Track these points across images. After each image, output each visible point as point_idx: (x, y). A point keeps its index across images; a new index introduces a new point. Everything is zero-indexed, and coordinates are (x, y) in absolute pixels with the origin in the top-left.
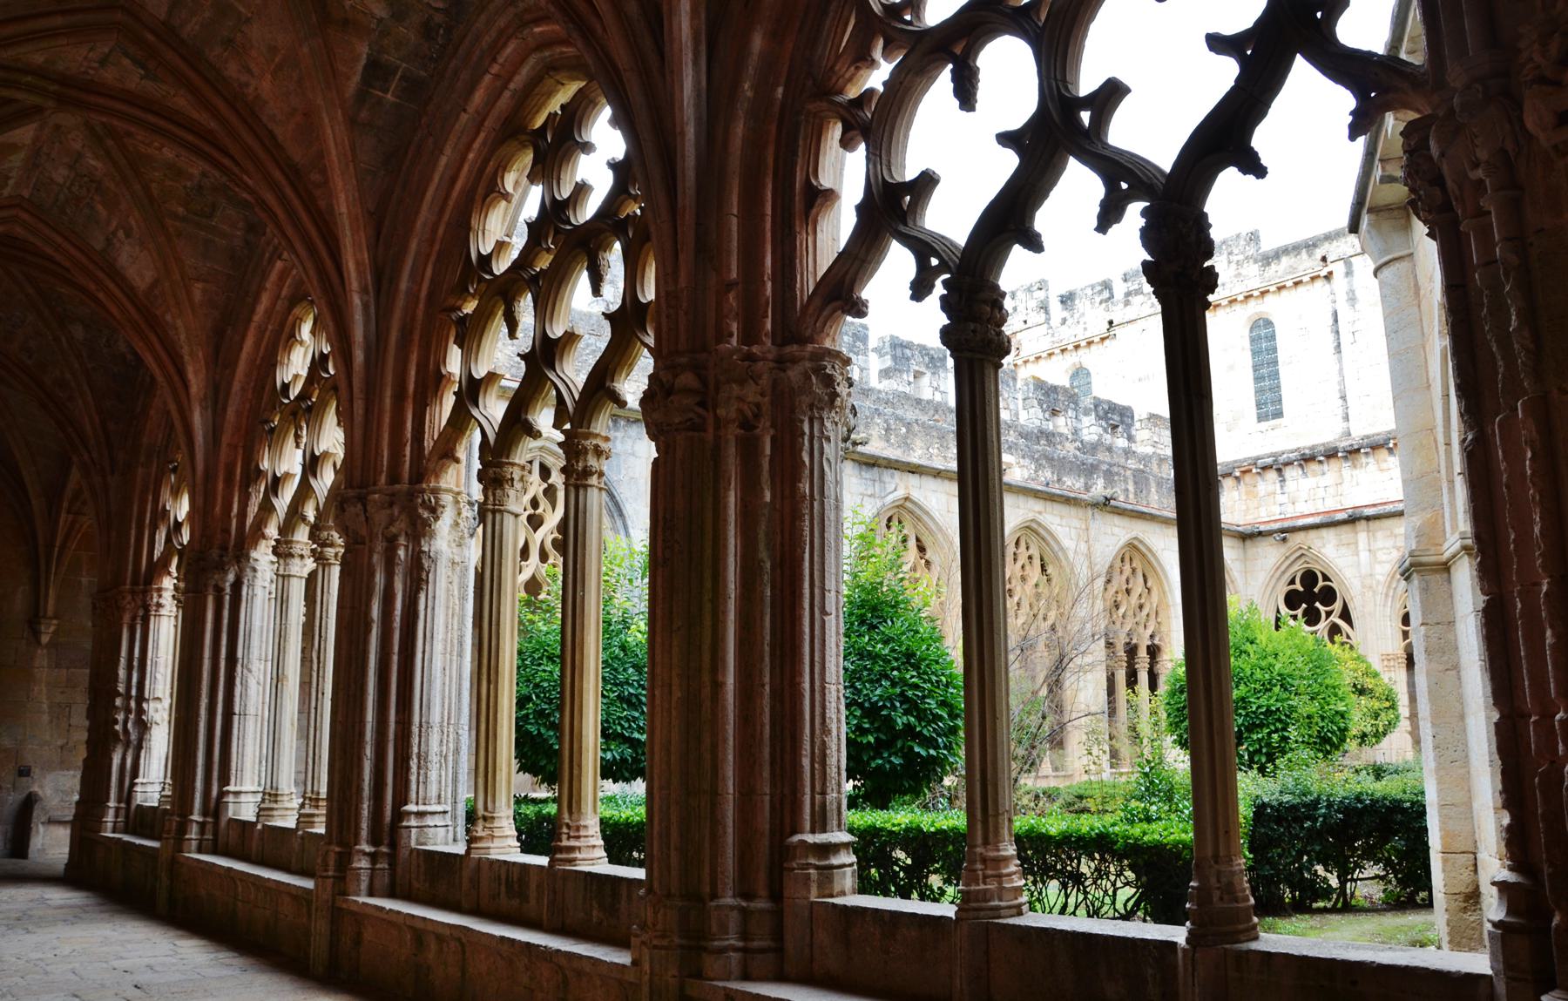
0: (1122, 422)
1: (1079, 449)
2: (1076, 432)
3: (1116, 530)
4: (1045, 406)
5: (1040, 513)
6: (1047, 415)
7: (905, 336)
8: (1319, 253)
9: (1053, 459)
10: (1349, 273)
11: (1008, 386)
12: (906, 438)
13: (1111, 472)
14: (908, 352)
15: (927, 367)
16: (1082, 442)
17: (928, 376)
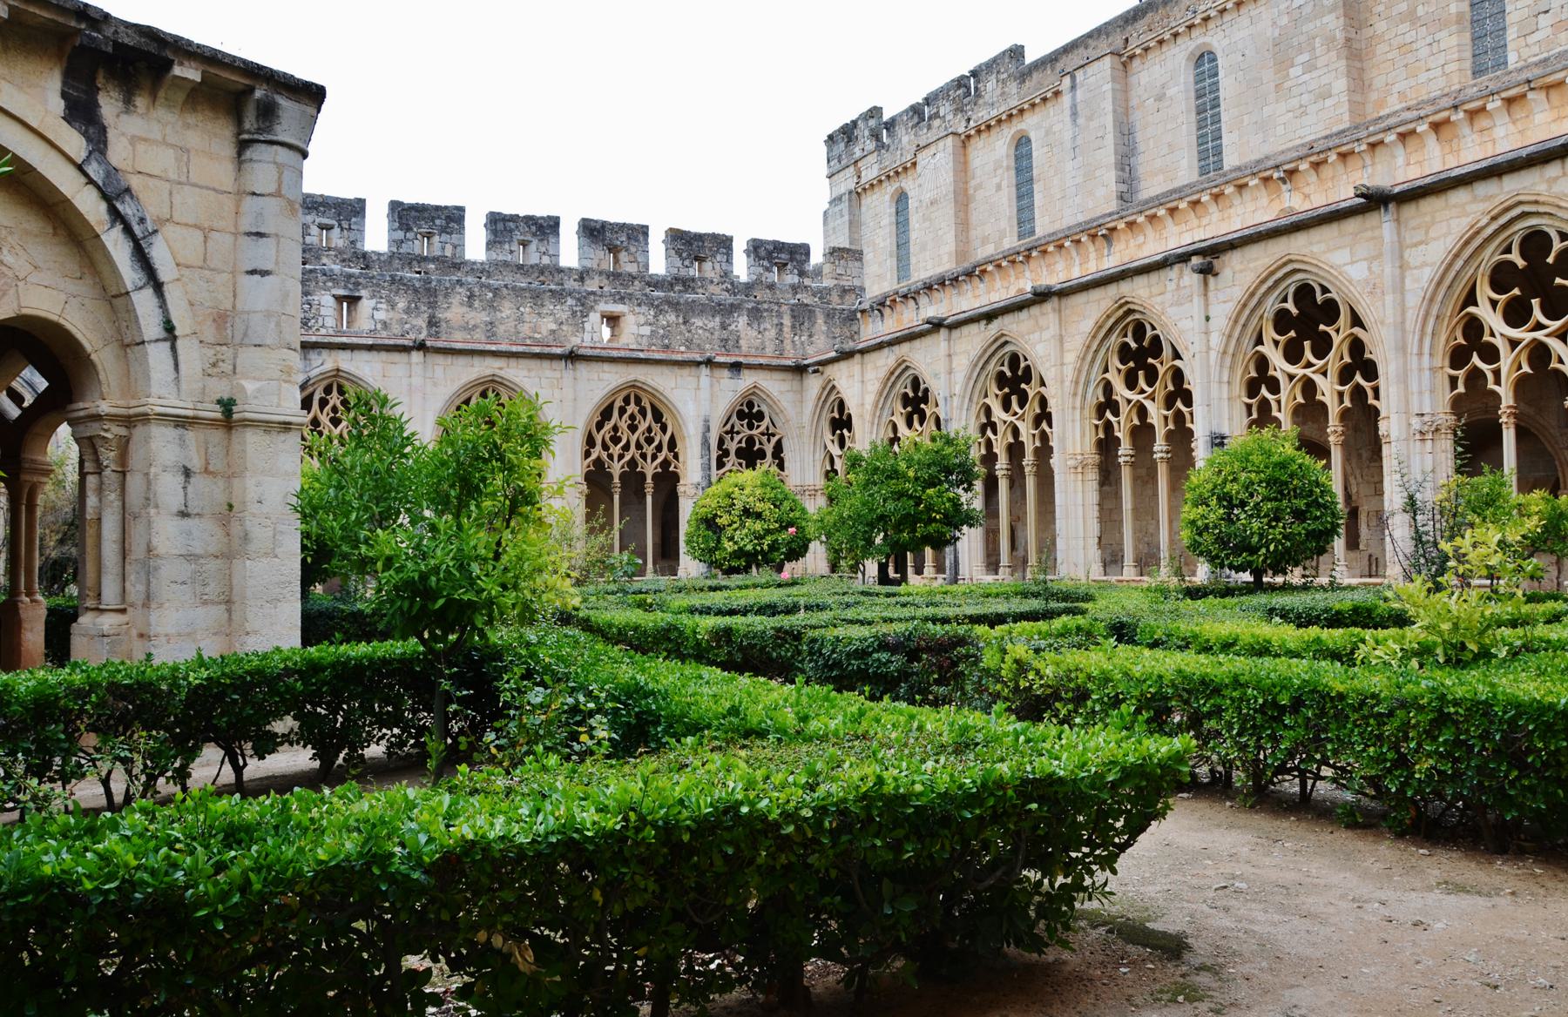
0: (792, 260)
1: (727, 290)
2: (726, 274)
3: (606, 376)
4: (684, 255)
5: (501, 369)
6: (687, 263)
7: (507, 210)
8: (1059, 66)
9: (678, 303)
10: (1073, 87)
11: (637, 241)
12: (493, 301)
13: (758, 310)
14: (512, 225)
15: (534, 235)
16: (732, 284)
17: (535, 242)
